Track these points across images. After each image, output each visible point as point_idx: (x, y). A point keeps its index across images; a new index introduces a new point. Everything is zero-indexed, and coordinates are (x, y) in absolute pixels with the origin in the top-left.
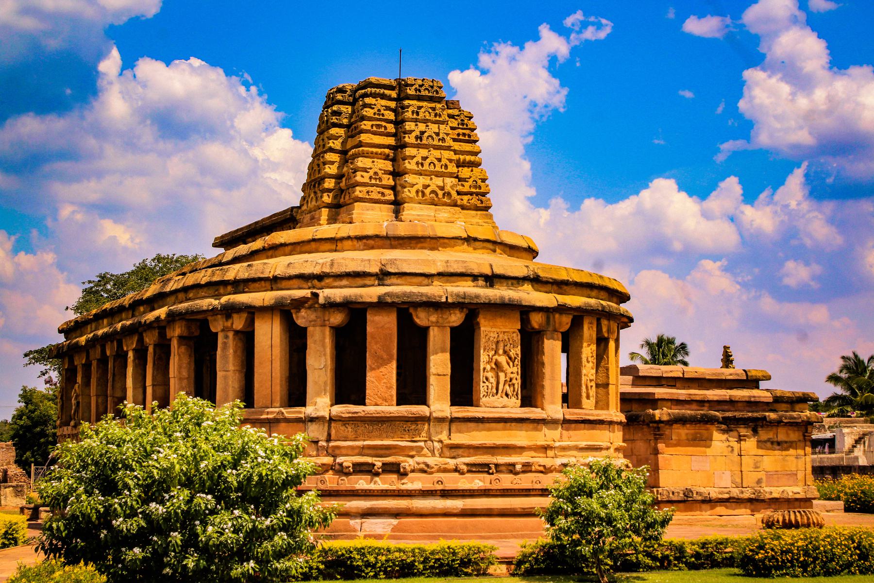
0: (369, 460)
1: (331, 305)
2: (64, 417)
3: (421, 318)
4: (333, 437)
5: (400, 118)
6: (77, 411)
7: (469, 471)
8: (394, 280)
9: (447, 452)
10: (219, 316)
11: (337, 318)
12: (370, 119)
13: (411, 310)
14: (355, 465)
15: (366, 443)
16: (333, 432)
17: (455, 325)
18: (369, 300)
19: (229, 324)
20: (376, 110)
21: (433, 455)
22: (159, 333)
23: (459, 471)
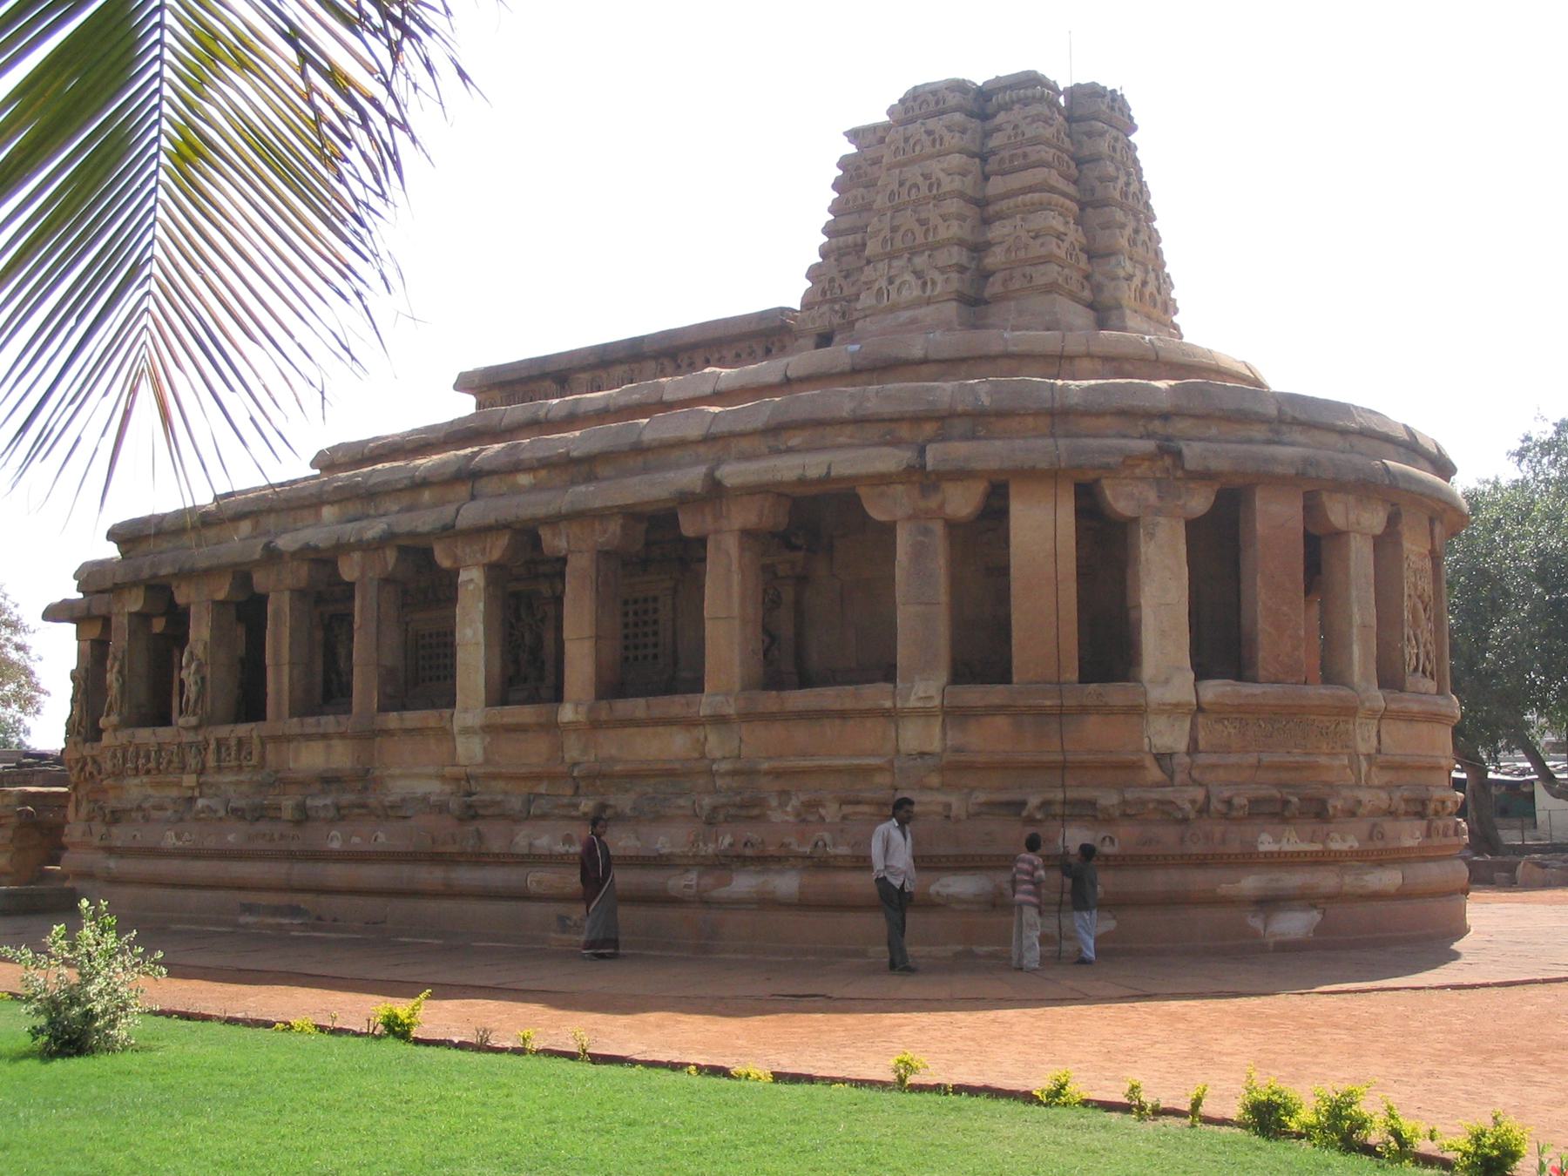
0: (1275, 792)
1: (1205, 476)
2: (125, 711)
3: (1338, 512)
4: (1202, 745)
5: (1086, 152)
6: (201, 694)
7: (1407, 813)
8: (1297, 436)
9: (1378, 778)
10: (900, 488)
11: (1199, 502)
12: (1047, 143)
13: (1325, 497)
14: (1254, 802)
15: (1267, 758)
16: (1201, 735)
17: (1379, 530)
18: (1279, 470)
19: (932, 503)
20: (1053, 130)
21: (1358, 785)
22: (623, 527)
23: (1391, 813)
